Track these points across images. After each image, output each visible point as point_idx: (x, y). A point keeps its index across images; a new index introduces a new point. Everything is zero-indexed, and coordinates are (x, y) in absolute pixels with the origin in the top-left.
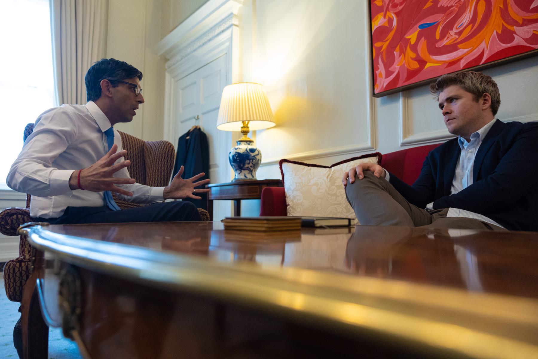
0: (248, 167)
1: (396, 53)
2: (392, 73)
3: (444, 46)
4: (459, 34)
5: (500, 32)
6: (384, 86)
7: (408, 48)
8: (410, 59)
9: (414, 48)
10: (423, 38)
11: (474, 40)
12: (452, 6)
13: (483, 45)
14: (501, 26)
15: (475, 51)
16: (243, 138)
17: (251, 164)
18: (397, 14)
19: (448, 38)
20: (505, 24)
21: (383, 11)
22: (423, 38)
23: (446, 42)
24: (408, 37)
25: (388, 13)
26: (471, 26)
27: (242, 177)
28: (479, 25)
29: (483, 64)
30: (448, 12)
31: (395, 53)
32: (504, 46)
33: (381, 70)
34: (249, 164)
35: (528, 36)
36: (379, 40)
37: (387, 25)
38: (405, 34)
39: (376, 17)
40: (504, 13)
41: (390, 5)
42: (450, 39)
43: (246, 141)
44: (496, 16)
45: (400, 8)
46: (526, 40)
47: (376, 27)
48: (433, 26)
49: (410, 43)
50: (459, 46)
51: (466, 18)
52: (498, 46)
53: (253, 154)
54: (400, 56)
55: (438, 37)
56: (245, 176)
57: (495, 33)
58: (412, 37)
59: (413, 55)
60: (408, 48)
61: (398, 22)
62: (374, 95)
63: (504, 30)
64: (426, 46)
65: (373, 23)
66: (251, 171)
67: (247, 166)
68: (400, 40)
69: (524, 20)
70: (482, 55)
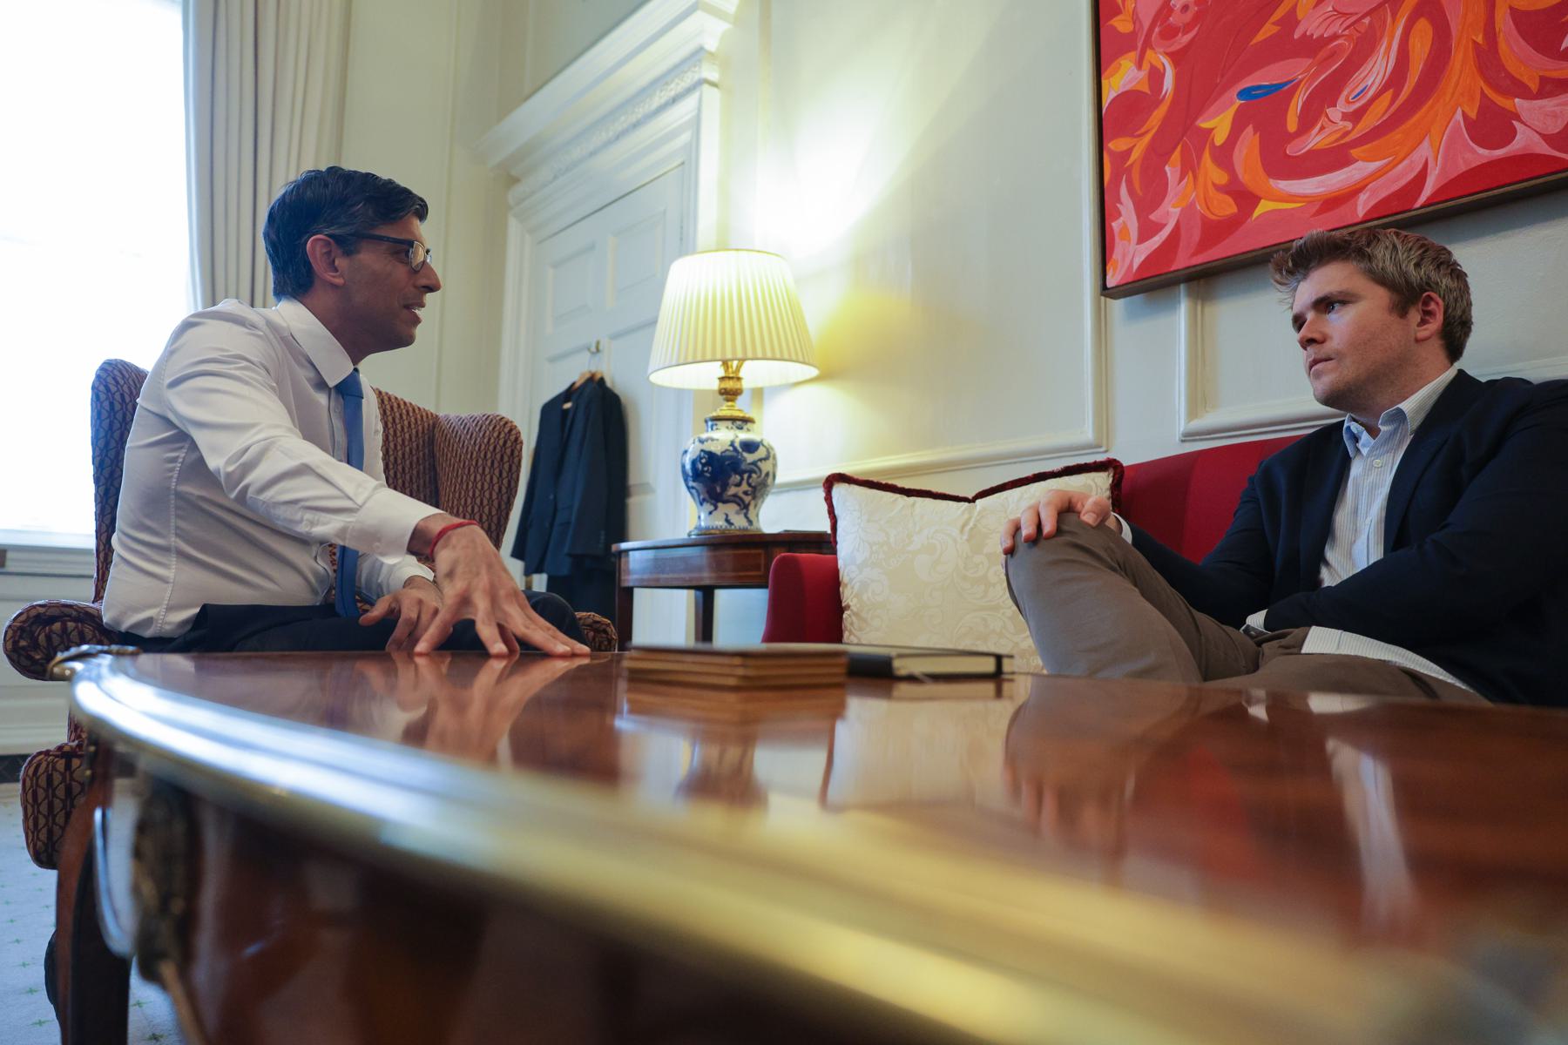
0: (735, 495)
1: (1171, 171)
2: (1159, 227)
5: (1473, 115)
6: (1135, 266)
8: (1212, 191)
9: (1224, 156)
10: (1250, 129)
11: (1397, 135)
12: (1335, 37)
13: (1424, 151)
14: (1478, 97)
15: (1400, 167)
16: (725, 410)
17: (745, 487)
18: (1176, 57)
19: (1323, 128)
20: (1488, 91)
21: (1134, 48)
22: (1250, 129)
23: (1315, 140)
24: (1205, 125)
25: (1149, 54)
26: (1388, 95)
27: (719, 522)
28: (1414, 94)
29: (1422, 207)
30: (1322, 54)
32: (1485, 154)
33: (1127, 218)
34: (739, 485)
35: (1554, 128)
36: (1119, 133)
37: (1146, 89)
38: (1196, 119)
40: (1487, 59)
42: (1327, 131)
43: (733, 420)
44: (1461, 65)
45: (1184, 39)
47: (1113, 95)
48: (1280, 94)
50: (1354, 152)
52: (1468, 156)
53: (750, 458)
54: (1181, 180)
55: (1292, 125)
56: (727, 521)
57: (1459, 116)
58: (1219, 124)
59: (1221, 177)
60: (1207, 155)
62: (1105, 290)
63: (1487, 107)
64: (1257, 151)
65: (1104, 82)
66: (744, 507)
67: (732, 490)
69: (1544, 80)
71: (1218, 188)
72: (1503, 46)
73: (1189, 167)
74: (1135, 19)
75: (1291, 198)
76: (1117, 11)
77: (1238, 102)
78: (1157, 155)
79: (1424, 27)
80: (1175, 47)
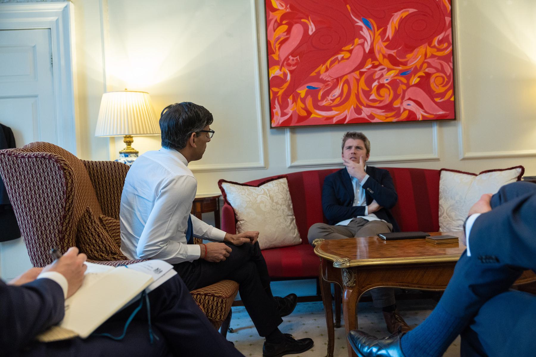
1: (290, 100)
3: (323, 106)
4: (333, 100)
7: (299, 100)
9: (303, 100)
10: (309, 96)
11: (341, 107)
12: (329, 81)
13: (346, 112)
18: (291, 72)
22: (309, 96)
23: (324, 103)
24: (299, 92)
25: (283, 68)
26: (339, 98)
28: (344, 99)
30: (326, 84)
32: (357, 116)
33: (277, 109)
35: (369, 114)
37: (282, 77)
39: (273, 67)
41: (285, 63)
44: (353, 97)
47: (273, 75)
50: (333, 108)
51: (337, 92)
54: (293, 103)
55: (319, 98)
57: (352, 107)
58: (302, 92)
59: (303, 106)
60: (299, 100)
61: (291, 77)
63: (357, 106)
64: (311, 102)
65: (270, 71)
68: (292, 91)
69: (367, 104)
70: (345, 118)
71: (302, 108)
73: (294, 101)
74: (279, 57)
76: (274, 53)
78: (286, 95)
79: (346, 86)
80: (291, 69)
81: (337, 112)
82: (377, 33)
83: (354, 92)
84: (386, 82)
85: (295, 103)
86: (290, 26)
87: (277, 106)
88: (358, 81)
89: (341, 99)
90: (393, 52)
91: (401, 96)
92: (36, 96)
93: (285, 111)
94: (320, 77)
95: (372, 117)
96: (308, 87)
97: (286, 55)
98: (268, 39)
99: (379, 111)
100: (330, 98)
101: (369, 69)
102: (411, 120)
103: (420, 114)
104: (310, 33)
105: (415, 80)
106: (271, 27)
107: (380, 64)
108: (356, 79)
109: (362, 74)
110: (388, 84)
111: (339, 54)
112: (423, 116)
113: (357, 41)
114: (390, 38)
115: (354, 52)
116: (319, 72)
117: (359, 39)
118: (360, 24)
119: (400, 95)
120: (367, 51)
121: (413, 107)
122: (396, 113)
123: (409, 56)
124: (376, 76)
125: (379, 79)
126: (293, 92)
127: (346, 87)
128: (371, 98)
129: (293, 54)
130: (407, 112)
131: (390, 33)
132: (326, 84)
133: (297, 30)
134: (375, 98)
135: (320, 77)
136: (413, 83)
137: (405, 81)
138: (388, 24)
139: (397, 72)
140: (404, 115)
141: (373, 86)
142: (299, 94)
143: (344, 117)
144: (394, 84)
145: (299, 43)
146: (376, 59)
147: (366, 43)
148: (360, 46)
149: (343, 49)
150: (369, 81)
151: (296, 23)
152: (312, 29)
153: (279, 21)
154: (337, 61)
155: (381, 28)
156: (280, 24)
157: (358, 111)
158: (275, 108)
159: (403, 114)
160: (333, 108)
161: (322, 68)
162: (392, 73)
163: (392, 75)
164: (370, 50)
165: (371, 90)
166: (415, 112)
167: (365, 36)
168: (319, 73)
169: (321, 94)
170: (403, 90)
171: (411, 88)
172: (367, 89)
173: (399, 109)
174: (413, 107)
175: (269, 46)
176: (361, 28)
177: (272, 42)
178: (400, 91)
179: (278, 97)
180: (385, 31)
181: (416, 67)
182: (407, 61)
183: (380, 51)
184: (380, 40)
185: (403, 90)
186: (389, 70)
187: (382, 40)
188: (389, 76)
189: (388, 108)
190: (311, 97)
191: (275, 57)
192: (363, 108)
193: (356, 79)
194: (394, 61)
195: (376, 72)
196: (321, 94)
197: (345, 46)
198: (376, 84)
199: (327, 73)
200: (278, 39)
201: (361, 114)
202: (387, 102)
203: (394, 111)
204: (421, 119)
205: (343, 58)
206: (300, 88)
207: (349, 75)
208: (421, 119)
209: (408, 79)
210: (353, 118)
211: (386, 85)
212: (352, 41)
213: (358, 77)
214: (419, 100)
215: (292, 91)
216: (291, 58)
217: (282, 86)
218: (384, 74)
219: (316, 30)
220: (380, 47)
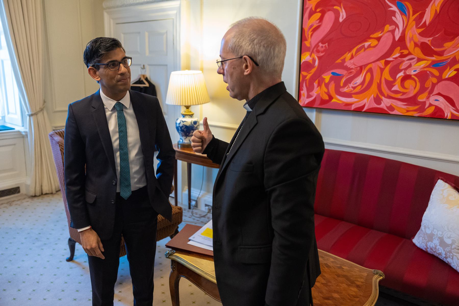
1: (316, 84)
4: (354, 88)
5: (375, 97)
7: (323, 85)
8: (324, 93)
9: (327, 85)
10: (333, 82)
11: (361, 95)
12: (352, 69)
13: (365, 101)
18: (319, 58)
21: (310, 51)
22: (333, 82)
23: (346, 90)
24: (324, 77)
25: (313, 55)
26: (360, 86)
30: (349, 71)
31: (315, 83)
32: (376, 106)
35: (388, 105)
36: (305, 70)
37: (311, 62)
38: (323, 73)
40: (379, 86)
41: (315, 49)
42: (349, 89)
44: (374, 86)
45: (322, 54)
46: (387, 107)
48: (339, 77)
49: (325, 82)
50: (353, 96)
51: (359, 80)
54: (318, 87)
55: (342, 85)
57: (372, 96)
58: (327, 77)
59: (326, 91)
60: (323, 85)
61: (319, 63)
63: (377, 95)
65: (302, 57)
68: (318, 76)
69: (388, 95)
70: (364, 106)
71: (325, 93)
72: (382, 85)
73: (319, 85)
74: (310, 44)
75: (339, 100)
76: (306, 40)
77: (332, 75)
79: (369, 74)
80: (319, 55)
81: (356, 100)
82: (412, 18)
83: (376, 80)
84: (413, 73)
85: (319, 87)
86: (323, 13)
87: (305, 88)
88: (382, 70)
89: (361, 88)
90: (427, 40)
91: (428, 91)
92: (167, 65)
93: (311, 93)
94: (345, 65)
95: (391, 108)
96: (332, 73)
97: (316, 43)
98: (303, 26)
99: (400, 104)
100: (351, 85)
101: (396, 58)
102: (437, 116)
103: (449, 111)
104: (341, 20)
105: (450, 73)
106: (306, 15)
107: (410, 54)
108: (381, 68)
109: (387, 63)
110: (414, 75)
111: (367, 41)
112: (452, 114)
113: (388, 28)
114: (427, 23)
115: (382, 40)
116: (345, 59)
117: (390, 25)
118: (394, 8)
119: (427, 88)
120: (397, 38)
121: (442, 103)
122: (419, 108)
123: (448, 45)
124: (403, 66)
125: (406, 69)
126: (319, 77)
127: (369, 75)
128: (394, 89)
129: (322, 41)
130: (433, 108)
131: (428, 17)
132: (349, 71)
133: (329, 17)
134: (398, 90)
135: (345, 65)
136: (447, 77)
137: (436, 73)
138: (427, 7)
139: (429, 62)
140: (430, 111)
141: (397, 77)
142: (324, 79)
143: (363, 105)
144: (423, 76)
145: (330, 30)
146: (406, 48)
147: (397, 29)
148: (390, 33)
149: (371, 36)
150: (394, 72)
151: (329, 10)
152: (343, 15)
153: (313, 9)
154: (363, 50)
155: (418, 12)
156: (315, 12)
157: (378, 100)
158: (302, 90)
159: (427, 110)
160: (353, 96)
161: (348, 56)
162: (422, 64)
163: (422, 66)
164: (400, 37)
165: (395, 80)
166: (444, 110)
167: (397, 22)
168: (344, 61)
169: (343, 80)
170: (433, 83)
171: (443, 82)
172: (391, 79)
173: (424, 103)
174: (442, 103)
175: (303, 34)
176: (394, 13)
177: (306, 29)
178: (428, 84)
179: (306, 80)
180: (422, 16)
181: (455, 58)
182: (444, 51)
183: (411, 39)
184: (415, 26)
185: (433, 83)
186: (419, 60)
187: (416, 27)
188: (418, 67)
189: (412, 101)
190: (335, 82)
191: (307, 43)
192: (383, 98)
193: (381, 68)
194: (426, 50)
195: (403, 61)
196: (343, 80)
197: (373, 33)
198: (401, 74)
199: (352, 61)
200: (311, 26)
201: (380, 104)
202: (411, 95)
203: (418, 105)
204: (449, 117)
205: (369, 46)
206: (326, 74)
207: (373, 64)
208: (449, 117)
209: (441, 71)
210: (371, 107)
211: (413, 76)
212: (381, 28)
213: (383, 66)
214: (451, 96)
215: (318, 76)
216: (320, 45)
217: (310, 70)
218: (412, 64)
219: (346, 18)
220: (414, 35)
